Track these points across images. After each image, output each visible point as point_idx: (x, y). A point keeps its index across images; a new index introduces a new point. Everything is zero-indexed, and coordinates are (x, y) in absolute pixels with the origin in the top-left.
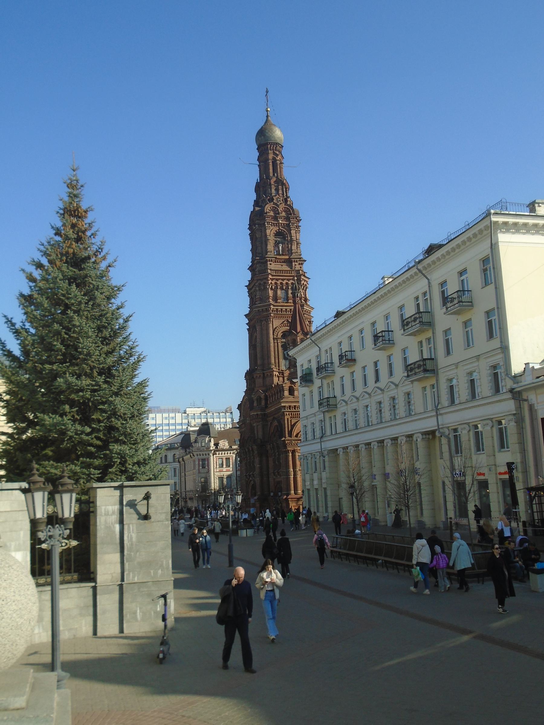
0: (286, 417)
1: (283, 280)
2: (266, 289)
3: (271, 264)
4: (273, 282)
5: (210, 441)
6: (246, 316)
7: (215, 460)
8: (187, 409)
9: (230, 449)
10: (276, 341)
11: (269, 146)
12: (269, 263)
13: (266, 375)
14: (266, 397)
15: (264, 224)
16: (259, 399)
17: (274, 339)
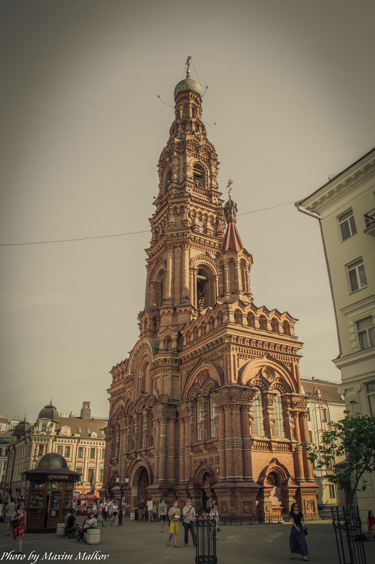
0: (232, 353)
1: (203, 209)
2: (182, 213)
3: (189, 190)
4: (192, 208)
5: (52, 425)
6: (146, 250)
7: (54, 447)
8: (12, 421)
9: (72, 437)
10: (192, 273)
11: (191, 94)
12: (187, 188)
13: (178, 310)
14: (180, 335)
15: (184, 152)
16: (169, 340)
17: (190, 268)
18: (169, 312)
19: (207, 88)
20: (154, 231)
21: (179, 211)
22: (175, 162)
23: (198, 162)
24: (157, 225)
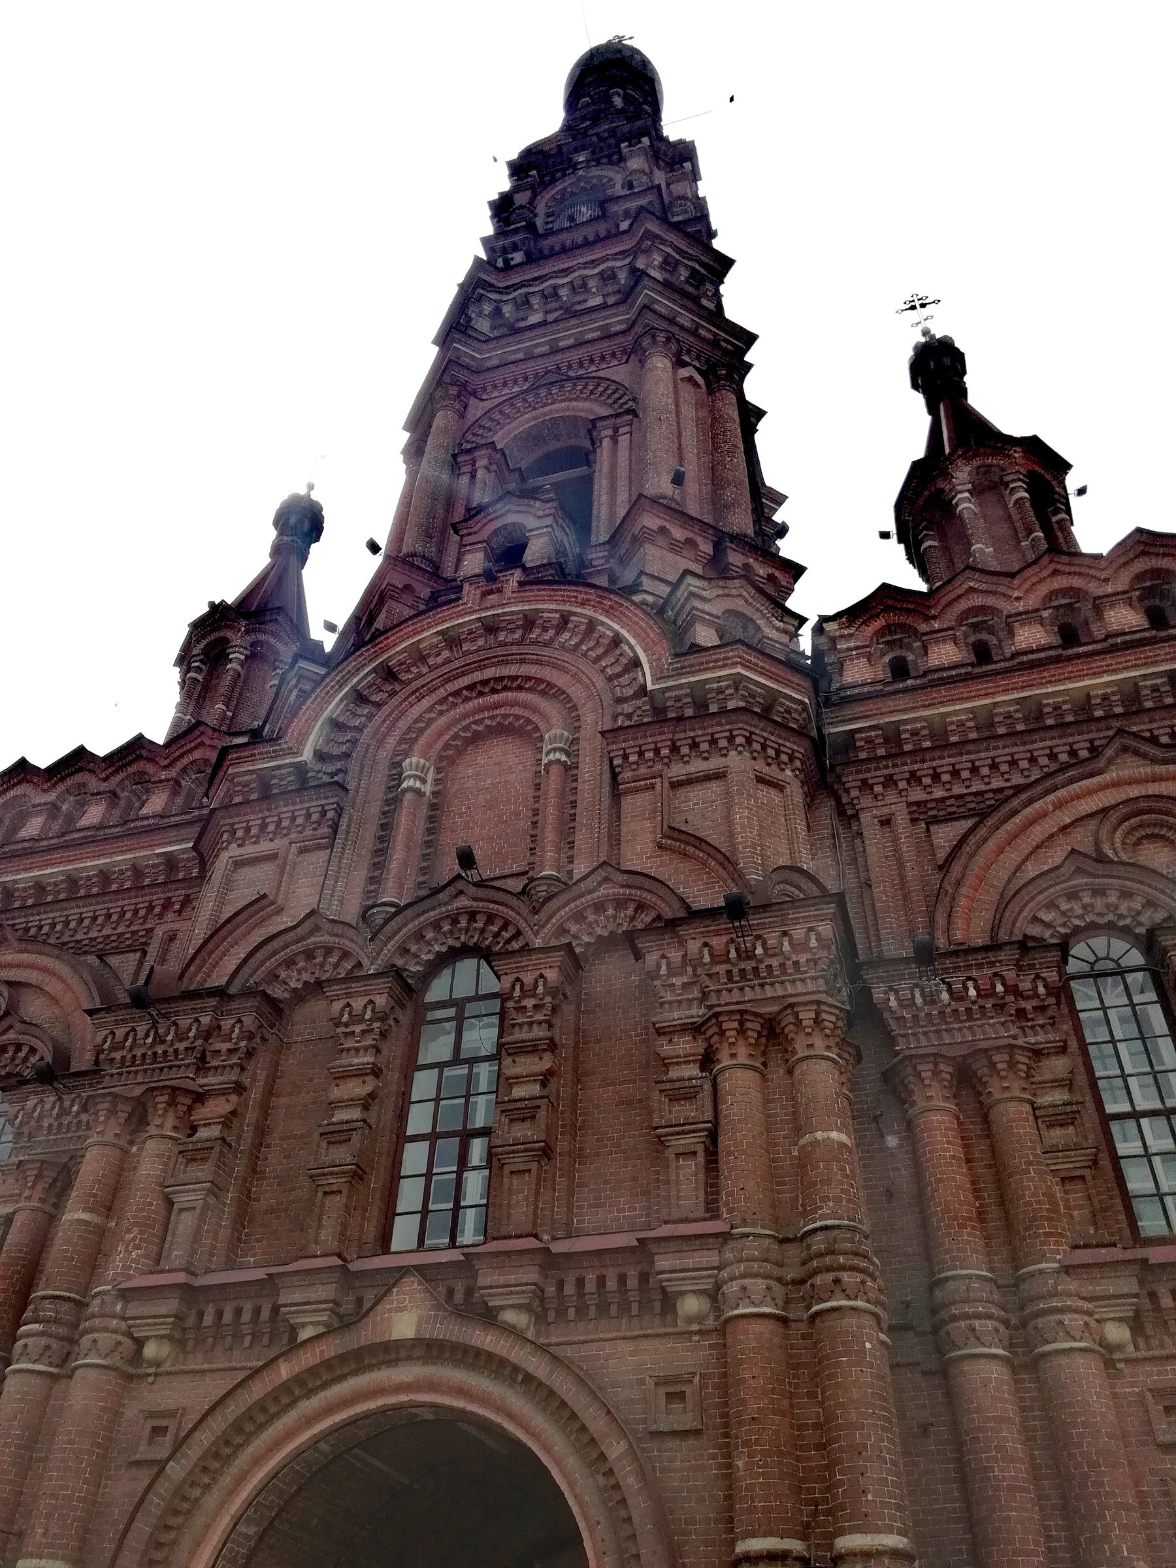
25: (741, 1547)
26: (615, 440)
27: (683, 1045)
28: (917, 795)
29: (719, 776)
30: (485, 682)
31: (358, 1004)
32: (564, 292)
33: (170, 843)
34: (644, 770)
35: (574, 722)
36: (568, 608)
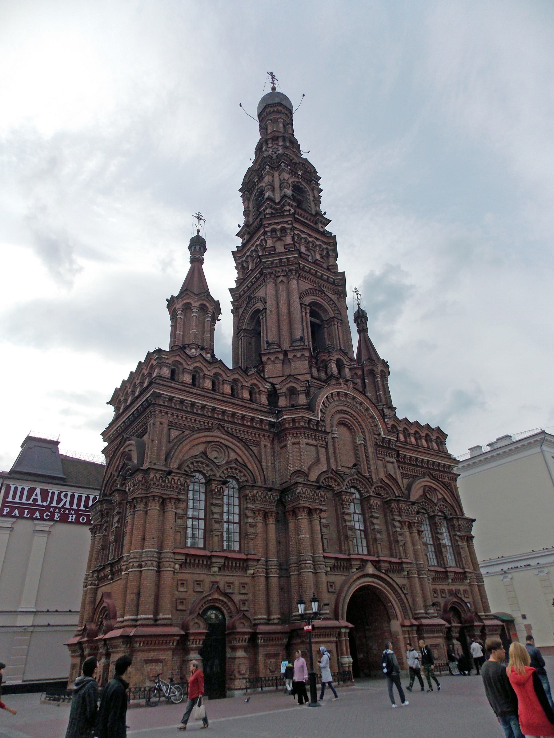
6: (231, 290)
10: (303, 310)
13: (290, 356)
18: (277, 358)
19: (304, 95)
20: (240, 267)
21: (278, 233)
22: (267, 179)
23: (297, 182)
24: (244, 259)
25: (418, 612)
26: (338, 326)
27: (397, 524)
28: (402, 471)
29: (392, 463)
30: (343, 410)
31: (348, 497)
32: (311, 245)
33: (262, 416)
34: (381, 456)
35: (363, 433)
36: (362, 400)
